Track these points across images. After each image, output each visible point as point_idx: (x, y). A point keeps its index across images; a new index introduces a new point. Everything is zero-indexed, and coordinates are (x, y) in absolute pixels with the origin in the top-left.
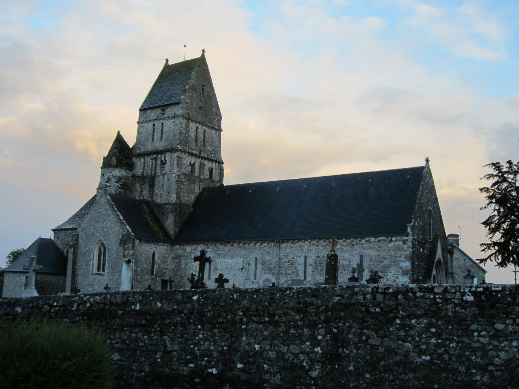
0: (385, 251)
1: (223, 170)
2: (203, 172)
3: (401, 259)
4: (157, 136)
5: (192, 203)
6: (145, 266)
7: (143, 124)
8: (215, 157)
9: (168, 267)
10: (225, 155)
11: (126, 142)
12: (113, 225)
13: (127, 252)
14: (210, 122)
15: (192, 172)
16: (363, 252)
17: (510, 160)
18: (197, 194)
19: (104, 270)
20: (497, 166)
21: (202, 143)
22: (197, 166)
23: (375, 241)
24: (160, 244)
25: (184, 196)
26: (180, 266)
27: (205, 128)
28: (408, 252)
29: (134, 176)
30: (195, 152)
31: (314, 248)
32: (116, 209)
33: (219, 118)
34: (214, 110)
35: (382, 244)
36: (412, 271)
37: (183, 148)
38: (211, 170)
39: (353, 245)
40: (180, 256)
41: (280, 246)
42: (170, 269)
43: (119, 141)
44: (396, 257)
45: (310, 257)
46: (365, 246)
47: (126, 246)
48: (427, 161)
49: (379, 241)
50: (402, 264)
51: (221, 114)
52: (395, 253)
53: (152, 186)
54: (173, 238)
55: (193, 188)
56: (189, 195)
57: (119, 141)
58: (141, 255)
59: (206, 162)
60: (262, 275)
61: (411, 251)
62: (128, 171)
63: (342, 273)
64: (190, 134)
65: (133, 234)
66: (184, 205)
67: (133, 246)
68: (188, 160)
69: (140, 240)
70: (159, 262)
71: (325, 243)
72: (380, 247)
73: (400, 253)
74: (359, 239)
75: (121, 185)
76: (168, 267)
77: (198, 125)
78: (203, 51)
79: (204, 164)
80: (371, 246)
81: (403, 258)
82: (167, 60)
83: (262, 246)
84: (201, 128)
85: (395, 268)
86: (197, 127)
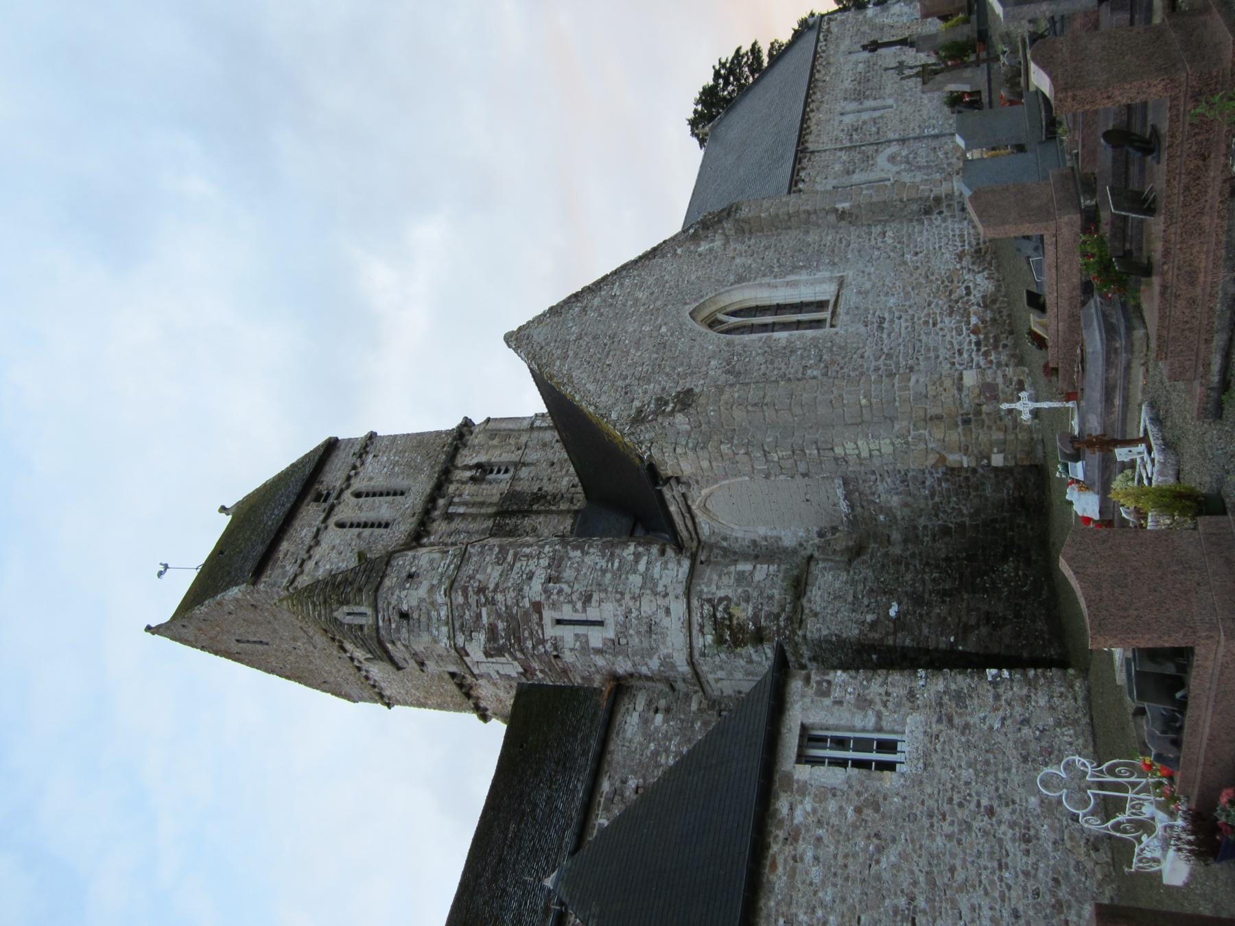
4: (383, 509)
12: (651, 280)
19: (821, 305)
39: (829, 63)
81: (861, 17)
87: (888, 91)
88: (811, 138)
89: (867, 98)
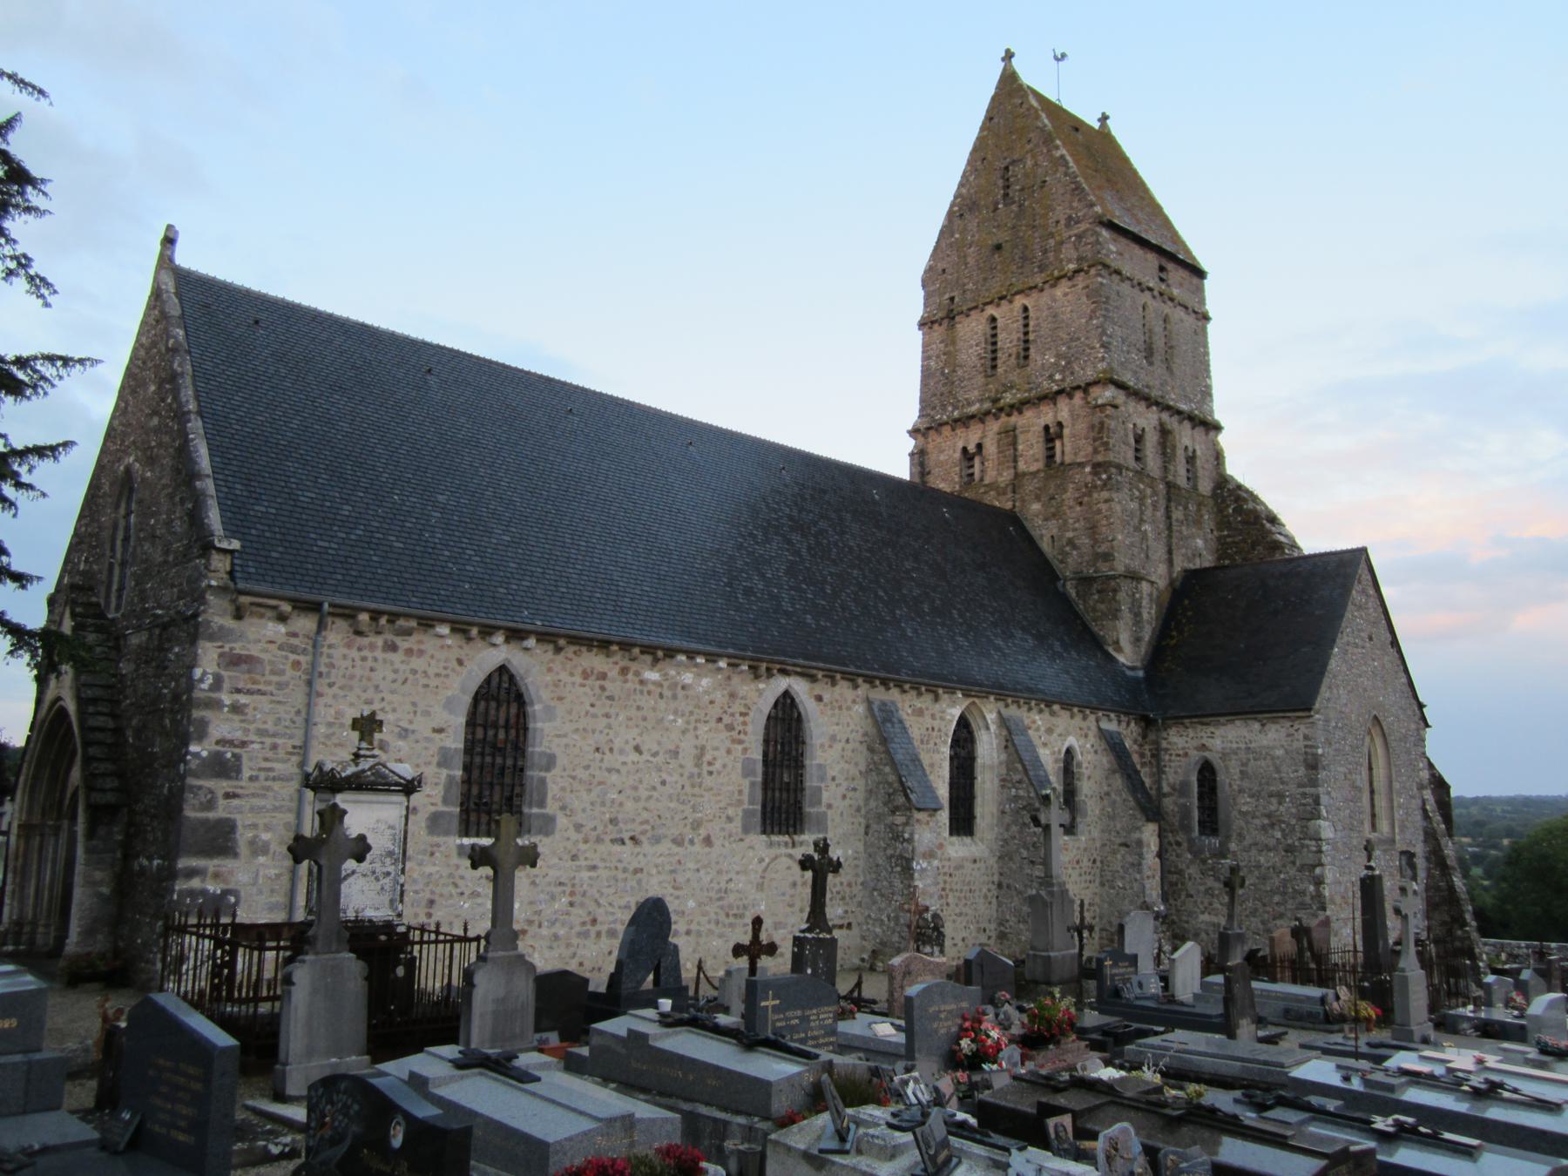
14: (1042, 268)
77: (990, 310)
84: (1006, 315)
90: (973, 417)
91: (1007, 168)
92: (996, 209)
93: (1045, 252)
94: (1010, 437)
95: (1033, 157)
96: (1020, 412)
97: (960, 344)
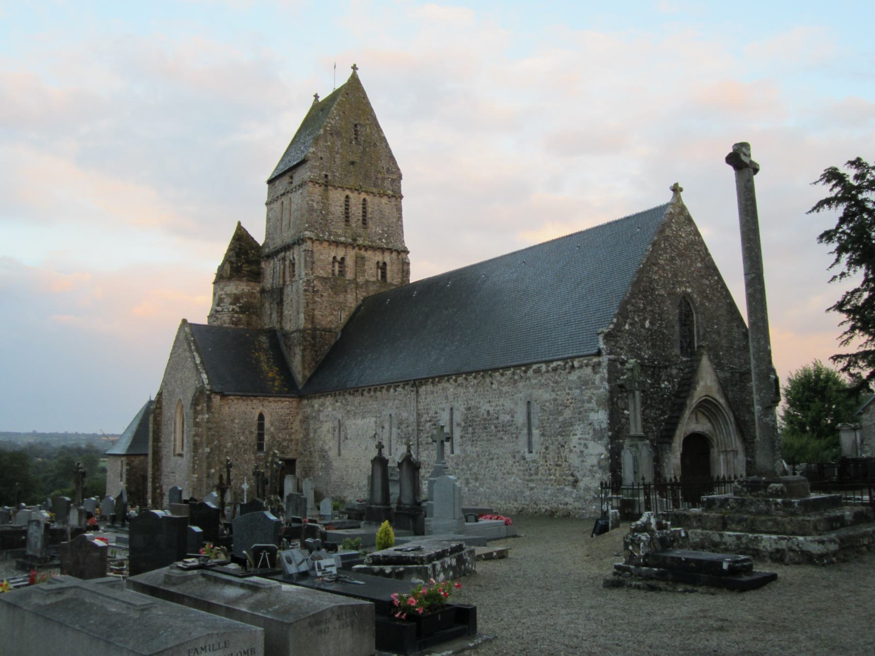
0: (565, 390)
1: (408, 264)
2: (364, 271)
3: (590, 405)
5: (341, 326)
6: (242, 438)
7: (272, 206)
8: (387, 243)
9: (293, 437)
10: (411, 239)
11: (252, 239)
13: (200, 417)
14: (375, 186)
15: (342, 273)
16: (530, 395)
17: (859, 159)
18: (353, 310)
20: (833, 175)
21: (360, 223)
22: (350, 262)
23: (547, 372)
24: (271, 399)
25: (322, 316)
26: (308, 434)
27: (363, 195)
28: (602, 390)
29: (263, 291)
30: (343, 239)
31: (461, 390)
32: (193, 348)
33: (394, 177)
34: (383, 164)
35: (559, 376)
36: (610, 430)
37: (317, 235)
38: (383, 267)
39: (515, 381)
40: (307, 418)
41: (417, 392)
42: (297, 440)
43: (241, 239)
44: (583, 402)
45: (458, 409)
46: (534, 381)
47: (199, 408)
48: (676, 189)
49: (555, 370)
50: (593, 416)
51: (398, 169)
52: (582, 394)
53: (281, 303)
54: (300, 387)
55: (341, 300)
56: (335, 313)
57: (241, 239)
58: (233, 421)
59: (368, 254)
60: (398, 446)
61: (607, 387)
62: (252, 284)
63: (502, 439)
64: (332, 209)
65: (208, 387)
66: (325, 330)
67: (209, 408)
68: (326, 254)
69: (223, 396)
70: (272, 429)
71: (476, 381)
72: (557, 382)
73: (588, 393)
74: (523, 368)
75: (240, 307)
76: (293, 437)
77: (348, 192)
78: (354, 68)
79: (363, 258)
80: (543, 381)
81: (593, 405)
82: (316, 96)
83: (396, 393)
84: (356, 199)
85: (582, 425)
86: (347, 197)
87: (469, 449)
88: (430, 387)
89: (465, 429)
90: (342, 243)
91: (356, 126)
92: (351, 143)
93: (377, 178)
94: (360, 261)
95: (370, 128)
96: (366, 250)
97: (331, 202)
